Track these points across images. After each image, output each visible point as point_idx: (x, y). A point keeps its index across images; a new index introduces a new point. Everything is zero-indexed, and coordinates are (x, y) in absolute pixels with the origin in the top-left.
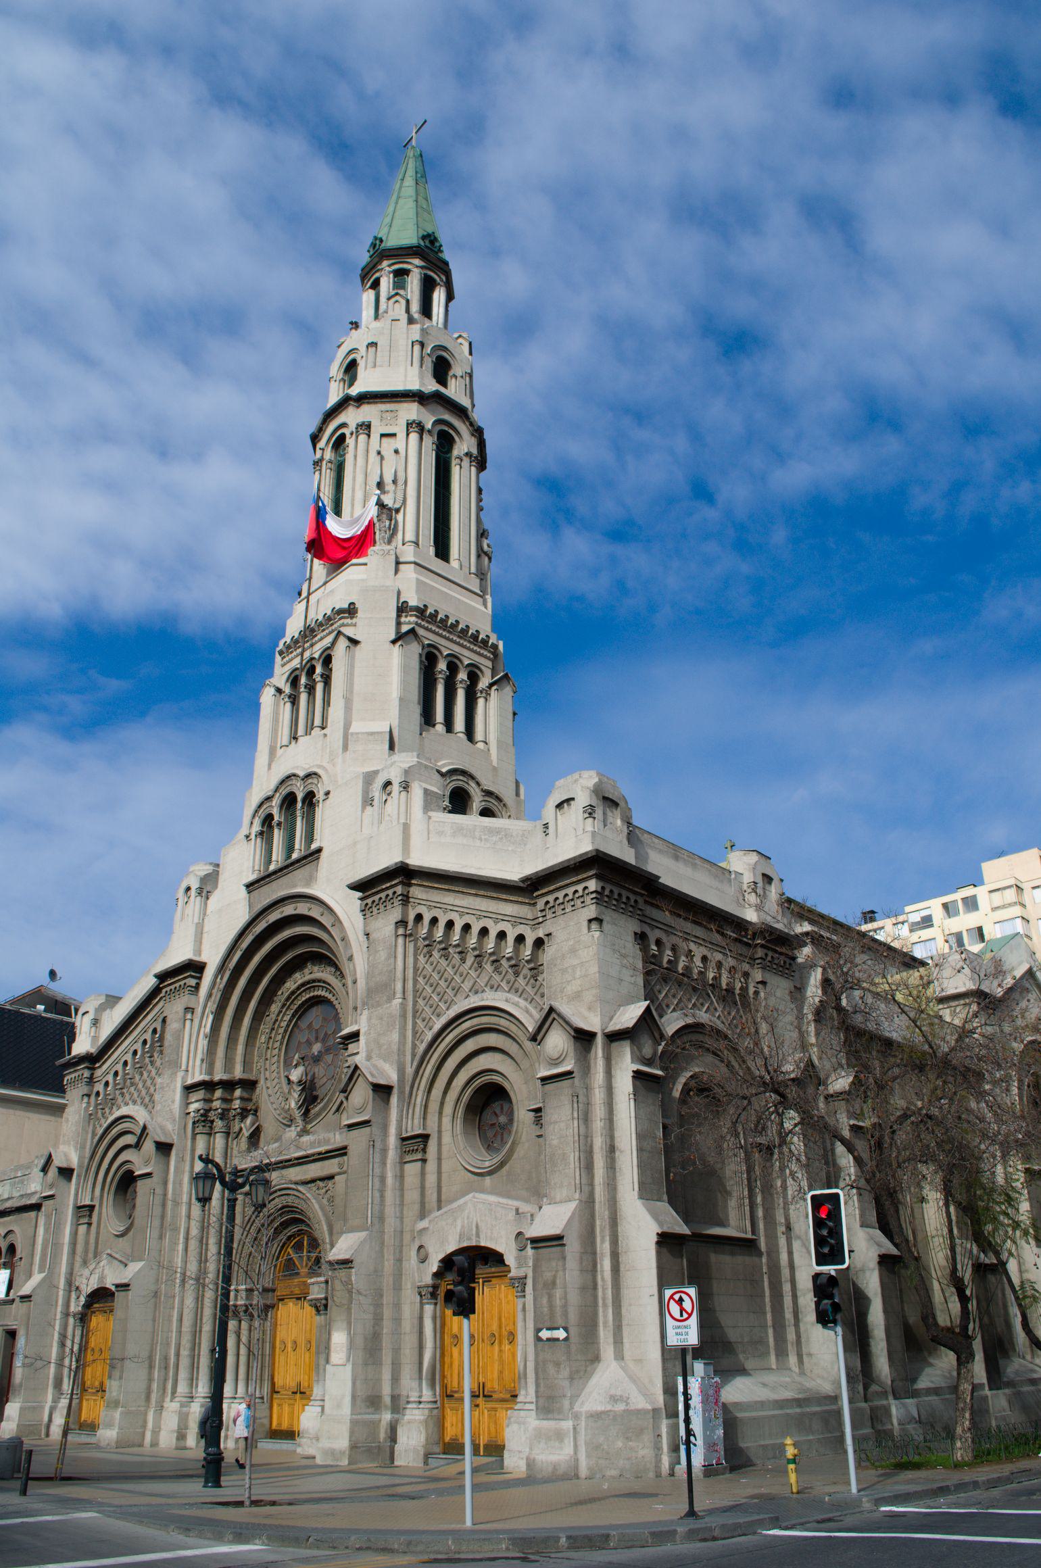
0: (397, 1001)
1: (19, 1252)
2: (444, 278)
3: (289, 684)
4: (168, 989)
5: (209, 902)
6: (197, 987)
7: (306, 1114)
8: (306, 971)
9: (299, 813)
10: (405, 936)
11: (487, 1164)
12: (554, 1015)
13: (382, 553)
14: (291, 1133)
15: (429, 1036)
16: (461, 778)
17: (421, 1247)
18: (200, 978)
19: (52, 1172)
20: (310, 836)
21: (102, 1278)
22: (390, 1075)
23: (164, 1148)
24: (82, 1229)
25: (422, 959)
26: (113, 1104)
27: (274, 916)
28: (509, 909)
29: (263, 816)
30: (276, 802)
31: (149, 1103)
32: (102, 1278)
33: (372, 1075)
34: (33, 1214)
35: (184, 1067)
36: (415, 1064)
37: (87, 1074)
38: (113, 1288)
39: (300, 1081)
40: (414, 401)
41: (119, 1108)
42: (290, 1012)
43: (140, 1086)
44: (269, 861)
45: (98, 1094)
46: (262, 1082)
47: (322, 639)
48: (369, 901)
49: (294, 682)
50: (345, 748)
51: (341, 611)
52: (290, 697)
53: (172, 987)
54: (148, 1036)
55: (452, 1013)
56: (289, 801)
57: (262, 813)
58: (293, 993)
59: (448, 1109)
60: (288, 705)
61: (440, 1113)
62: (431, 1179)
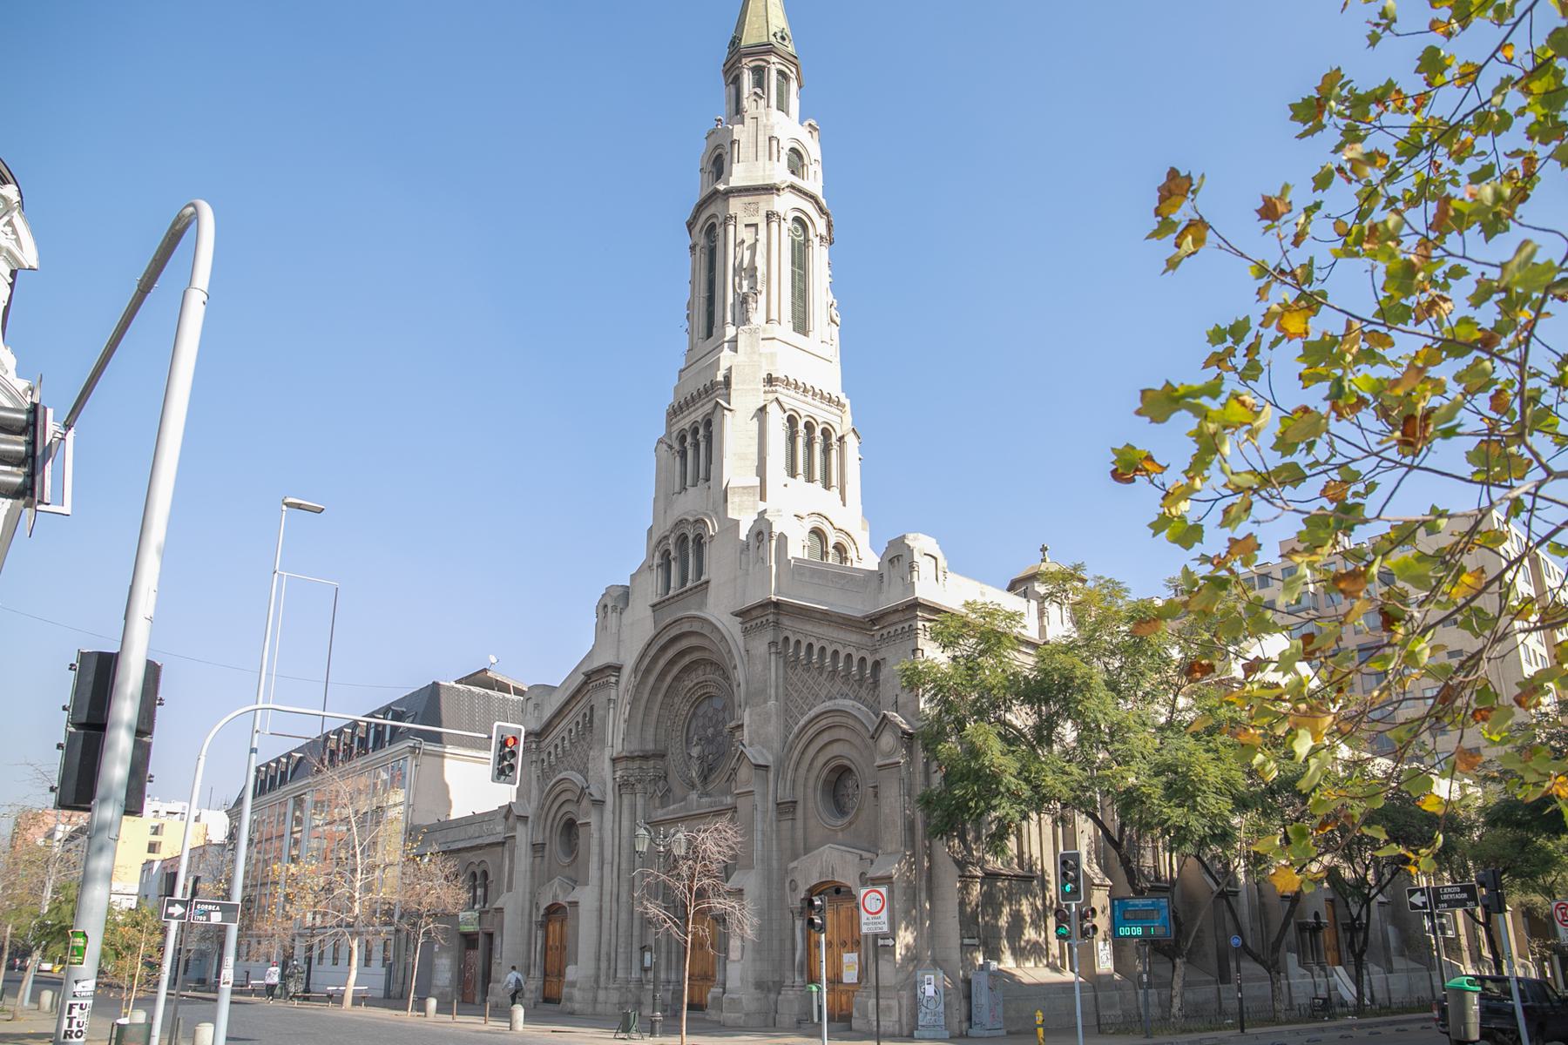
0: (772, 703)
1: (491, 877)
2: (794, 70)
4: (594, 684)
6: (617, 683)
8: (700, 672)
9: (690, 551)
11: (840, 823)
12: (886, 721)
14: (694, 796)
15: (796, 729)
17: (792, 881)
18: (618, 676)
19: (511, 819)
20: (700, 571)
21: (555, 896)
22: (767, 758)
23: (599, 803)
24: (538, 860)
25: (790, 673)
27: (674, 632)
28: (854, 638)
30: (671, 540)
31: (584, 772)
32: (555, 896)
33: (754, 757)
36: (785, 750)
38: (566, 905)
41: (561, 772)
42: (688, 705)
43: (576, 756)
44: (668, 588)
46: (670, 755)
47: (703, 405)
48: (748, 625)
49: (683, 439)
53: (598, 682)
54: (580, 719)
55: (812, 713)
56: (683, 539)
58: (690, 689)
59: (811, 783)
60: (678, 459)
61: (805, 786)
62: (800, 833)
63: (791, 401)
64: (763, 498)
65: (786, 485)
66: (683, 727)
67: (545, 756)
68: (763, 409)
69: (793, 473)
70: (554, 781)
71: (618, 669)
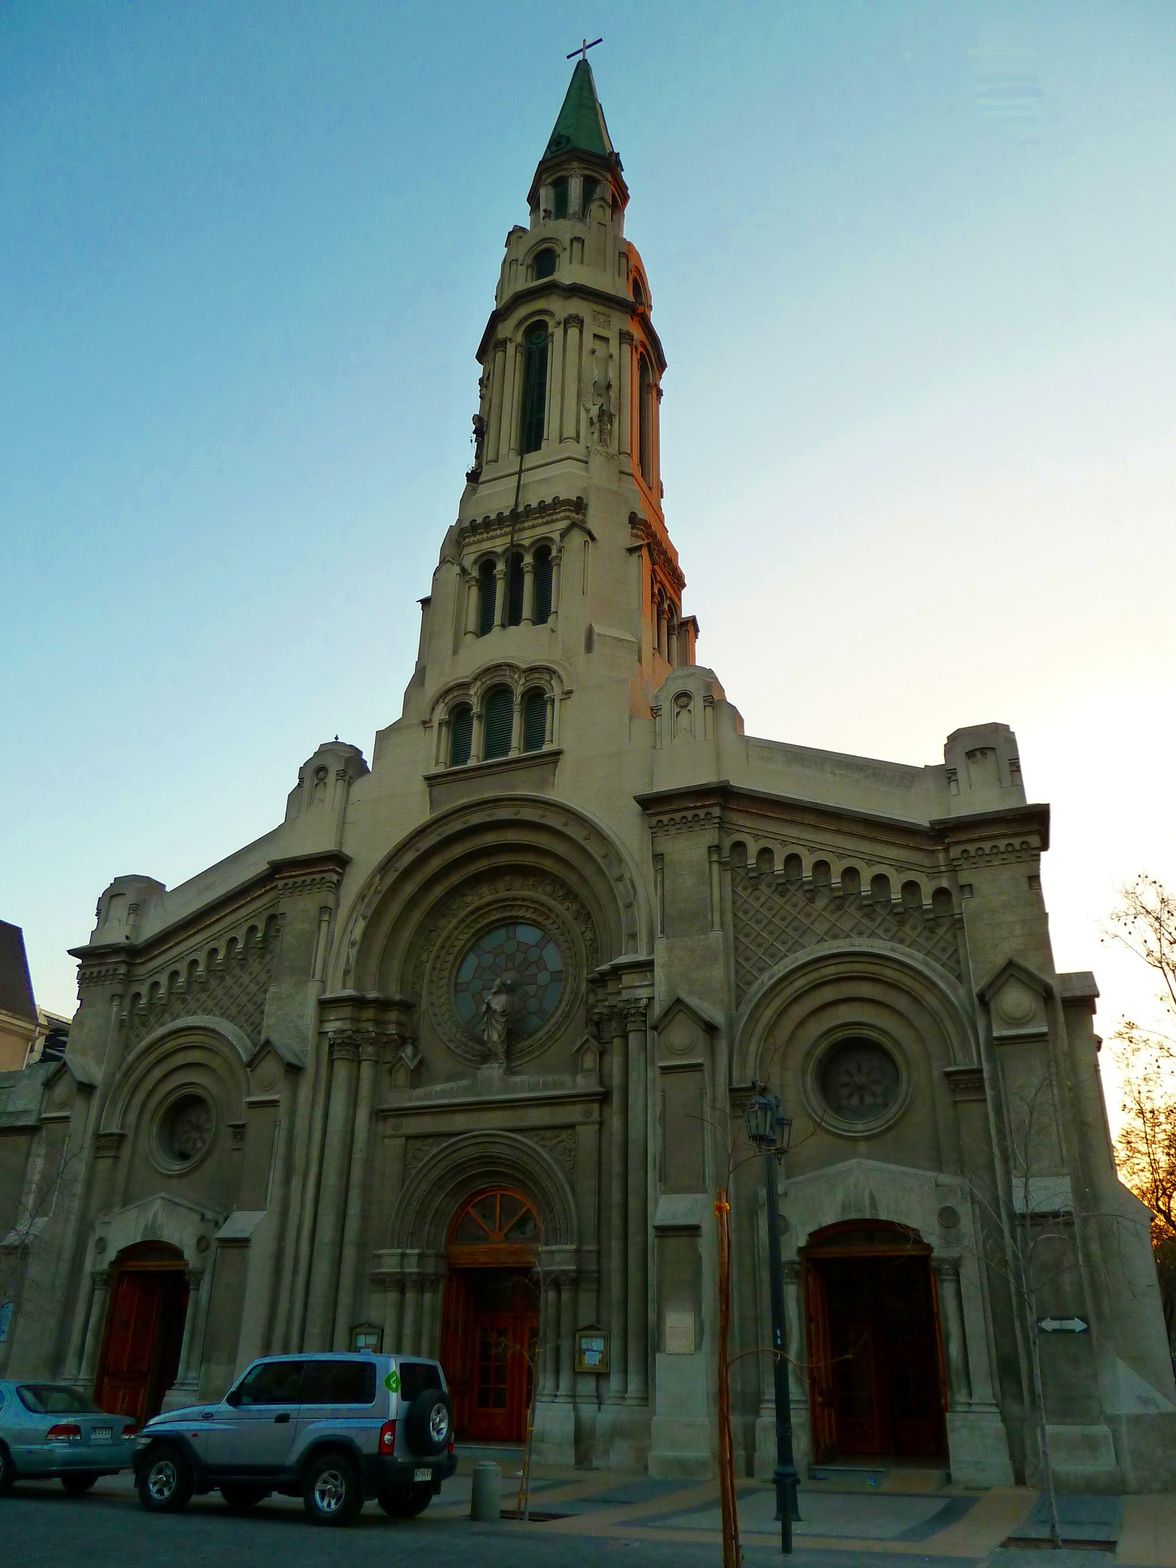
3: (477, 567)
5: (351, 789)
7: (508, 1054)
10: (720, 863)
14: (494, 1071)
20: (534, 736)
23: (293, 1070)
26: (163, 1012)
29: (451, 704)
31: (251, 1017)
34: (22, 1140)
35: (318, 976)
37: (122, 970)
39: (504, 1012)
40: (627, 313)
43: (220, 992)
45: (137, 996)
46: (424, 1003)
47: (534, 526)
49: (487, 564)
50: (589, 648)
51: (567, 502)
52: (477, 580)
56: (497, 695)
58: (479, 908)
60: (474, 591)
66: (453, 965)
67: (144, 990)
70: (160, 1031)
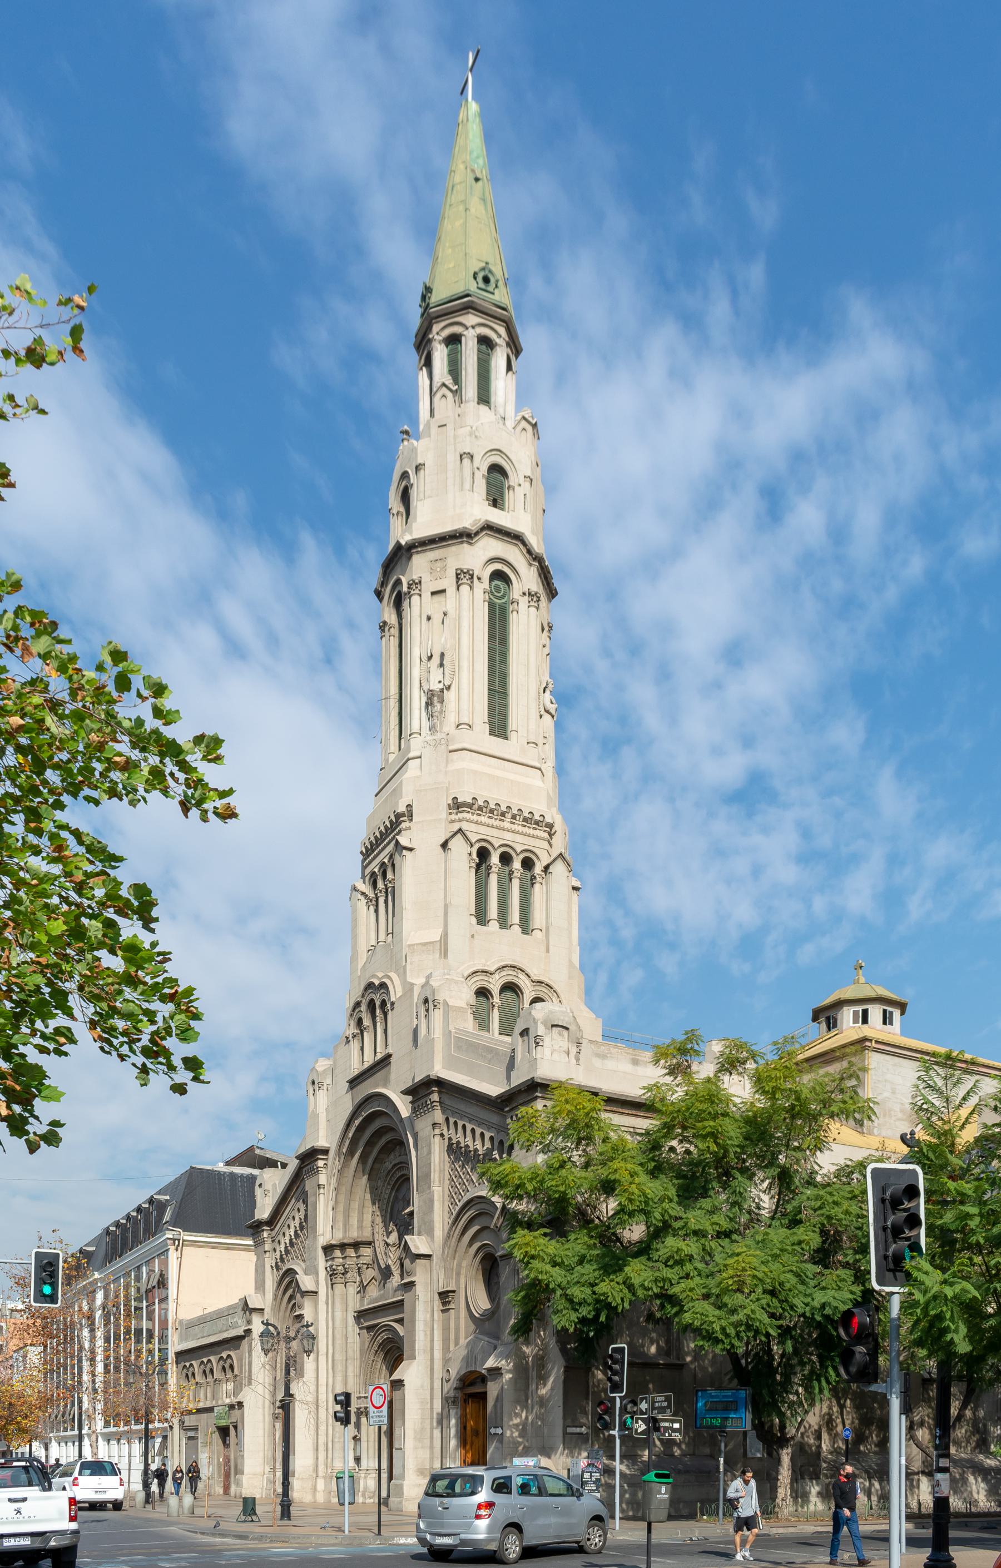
13: (432, 743)
16: (511, 972)
30: (363, 1007)
57: (356, 1017)
63: (483, 830)
64: (445, 954)
65: (473, 936)
68: (444, 845)
69: (481, 917)
71: (325, 1152)
